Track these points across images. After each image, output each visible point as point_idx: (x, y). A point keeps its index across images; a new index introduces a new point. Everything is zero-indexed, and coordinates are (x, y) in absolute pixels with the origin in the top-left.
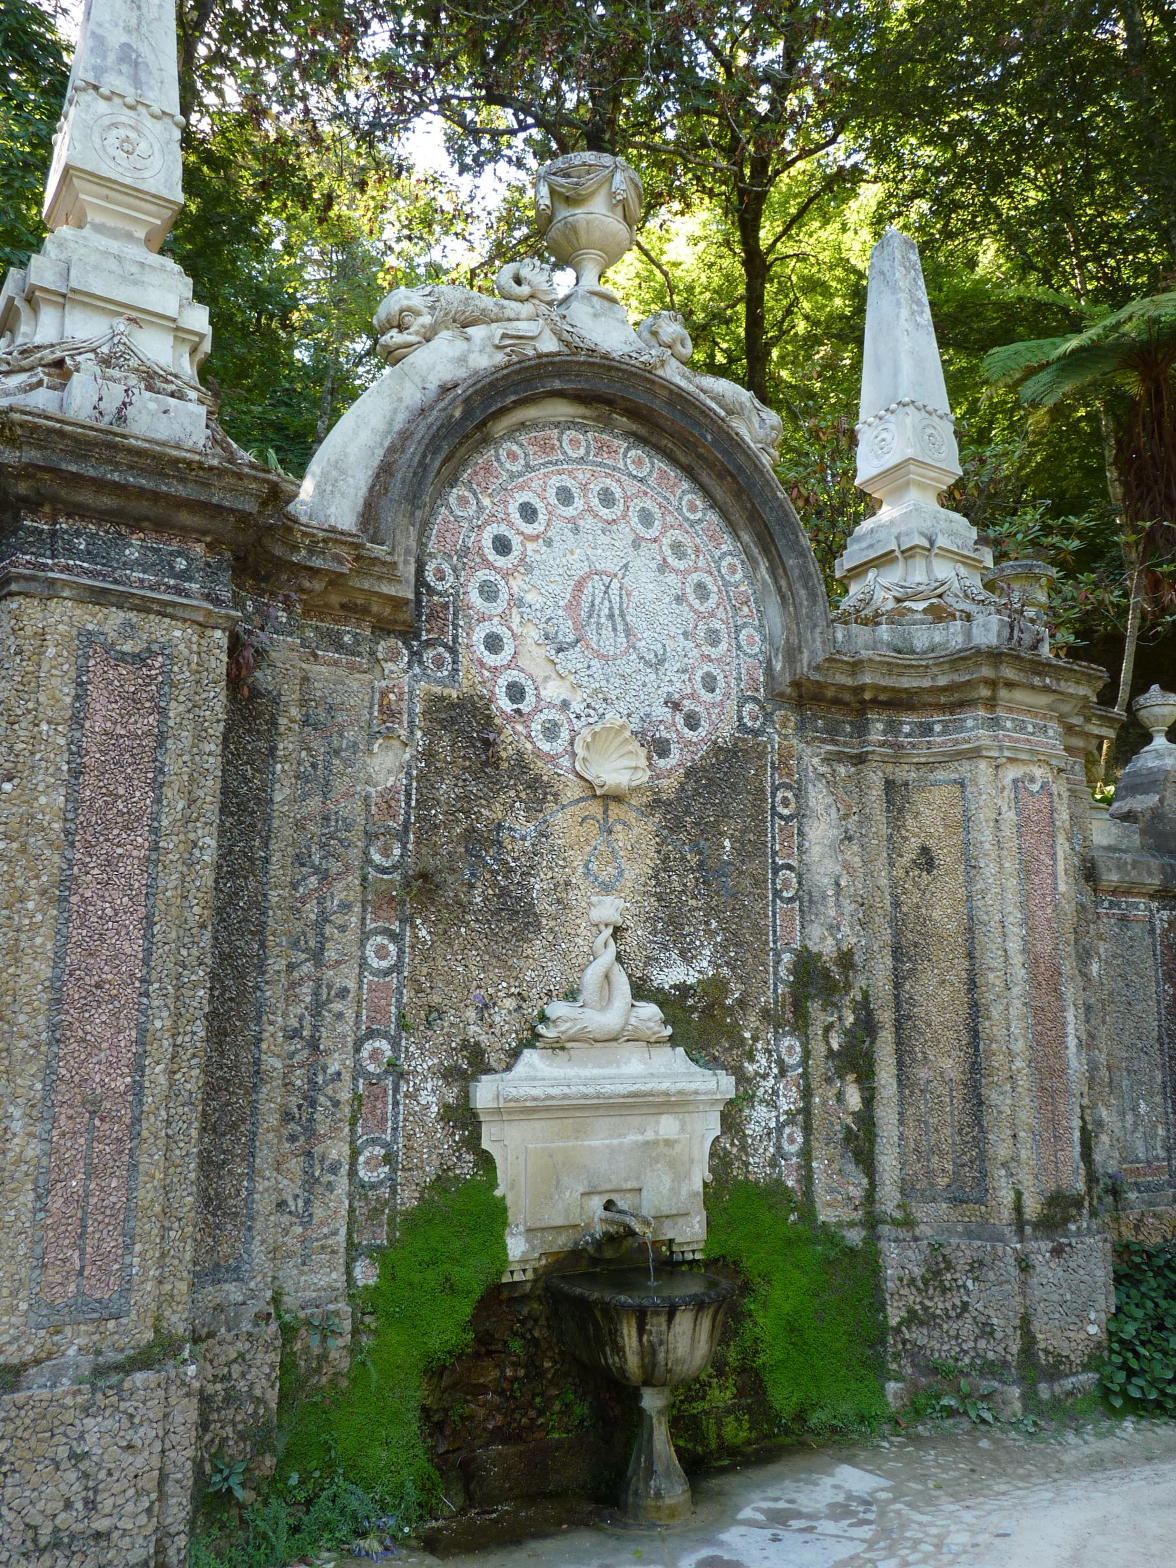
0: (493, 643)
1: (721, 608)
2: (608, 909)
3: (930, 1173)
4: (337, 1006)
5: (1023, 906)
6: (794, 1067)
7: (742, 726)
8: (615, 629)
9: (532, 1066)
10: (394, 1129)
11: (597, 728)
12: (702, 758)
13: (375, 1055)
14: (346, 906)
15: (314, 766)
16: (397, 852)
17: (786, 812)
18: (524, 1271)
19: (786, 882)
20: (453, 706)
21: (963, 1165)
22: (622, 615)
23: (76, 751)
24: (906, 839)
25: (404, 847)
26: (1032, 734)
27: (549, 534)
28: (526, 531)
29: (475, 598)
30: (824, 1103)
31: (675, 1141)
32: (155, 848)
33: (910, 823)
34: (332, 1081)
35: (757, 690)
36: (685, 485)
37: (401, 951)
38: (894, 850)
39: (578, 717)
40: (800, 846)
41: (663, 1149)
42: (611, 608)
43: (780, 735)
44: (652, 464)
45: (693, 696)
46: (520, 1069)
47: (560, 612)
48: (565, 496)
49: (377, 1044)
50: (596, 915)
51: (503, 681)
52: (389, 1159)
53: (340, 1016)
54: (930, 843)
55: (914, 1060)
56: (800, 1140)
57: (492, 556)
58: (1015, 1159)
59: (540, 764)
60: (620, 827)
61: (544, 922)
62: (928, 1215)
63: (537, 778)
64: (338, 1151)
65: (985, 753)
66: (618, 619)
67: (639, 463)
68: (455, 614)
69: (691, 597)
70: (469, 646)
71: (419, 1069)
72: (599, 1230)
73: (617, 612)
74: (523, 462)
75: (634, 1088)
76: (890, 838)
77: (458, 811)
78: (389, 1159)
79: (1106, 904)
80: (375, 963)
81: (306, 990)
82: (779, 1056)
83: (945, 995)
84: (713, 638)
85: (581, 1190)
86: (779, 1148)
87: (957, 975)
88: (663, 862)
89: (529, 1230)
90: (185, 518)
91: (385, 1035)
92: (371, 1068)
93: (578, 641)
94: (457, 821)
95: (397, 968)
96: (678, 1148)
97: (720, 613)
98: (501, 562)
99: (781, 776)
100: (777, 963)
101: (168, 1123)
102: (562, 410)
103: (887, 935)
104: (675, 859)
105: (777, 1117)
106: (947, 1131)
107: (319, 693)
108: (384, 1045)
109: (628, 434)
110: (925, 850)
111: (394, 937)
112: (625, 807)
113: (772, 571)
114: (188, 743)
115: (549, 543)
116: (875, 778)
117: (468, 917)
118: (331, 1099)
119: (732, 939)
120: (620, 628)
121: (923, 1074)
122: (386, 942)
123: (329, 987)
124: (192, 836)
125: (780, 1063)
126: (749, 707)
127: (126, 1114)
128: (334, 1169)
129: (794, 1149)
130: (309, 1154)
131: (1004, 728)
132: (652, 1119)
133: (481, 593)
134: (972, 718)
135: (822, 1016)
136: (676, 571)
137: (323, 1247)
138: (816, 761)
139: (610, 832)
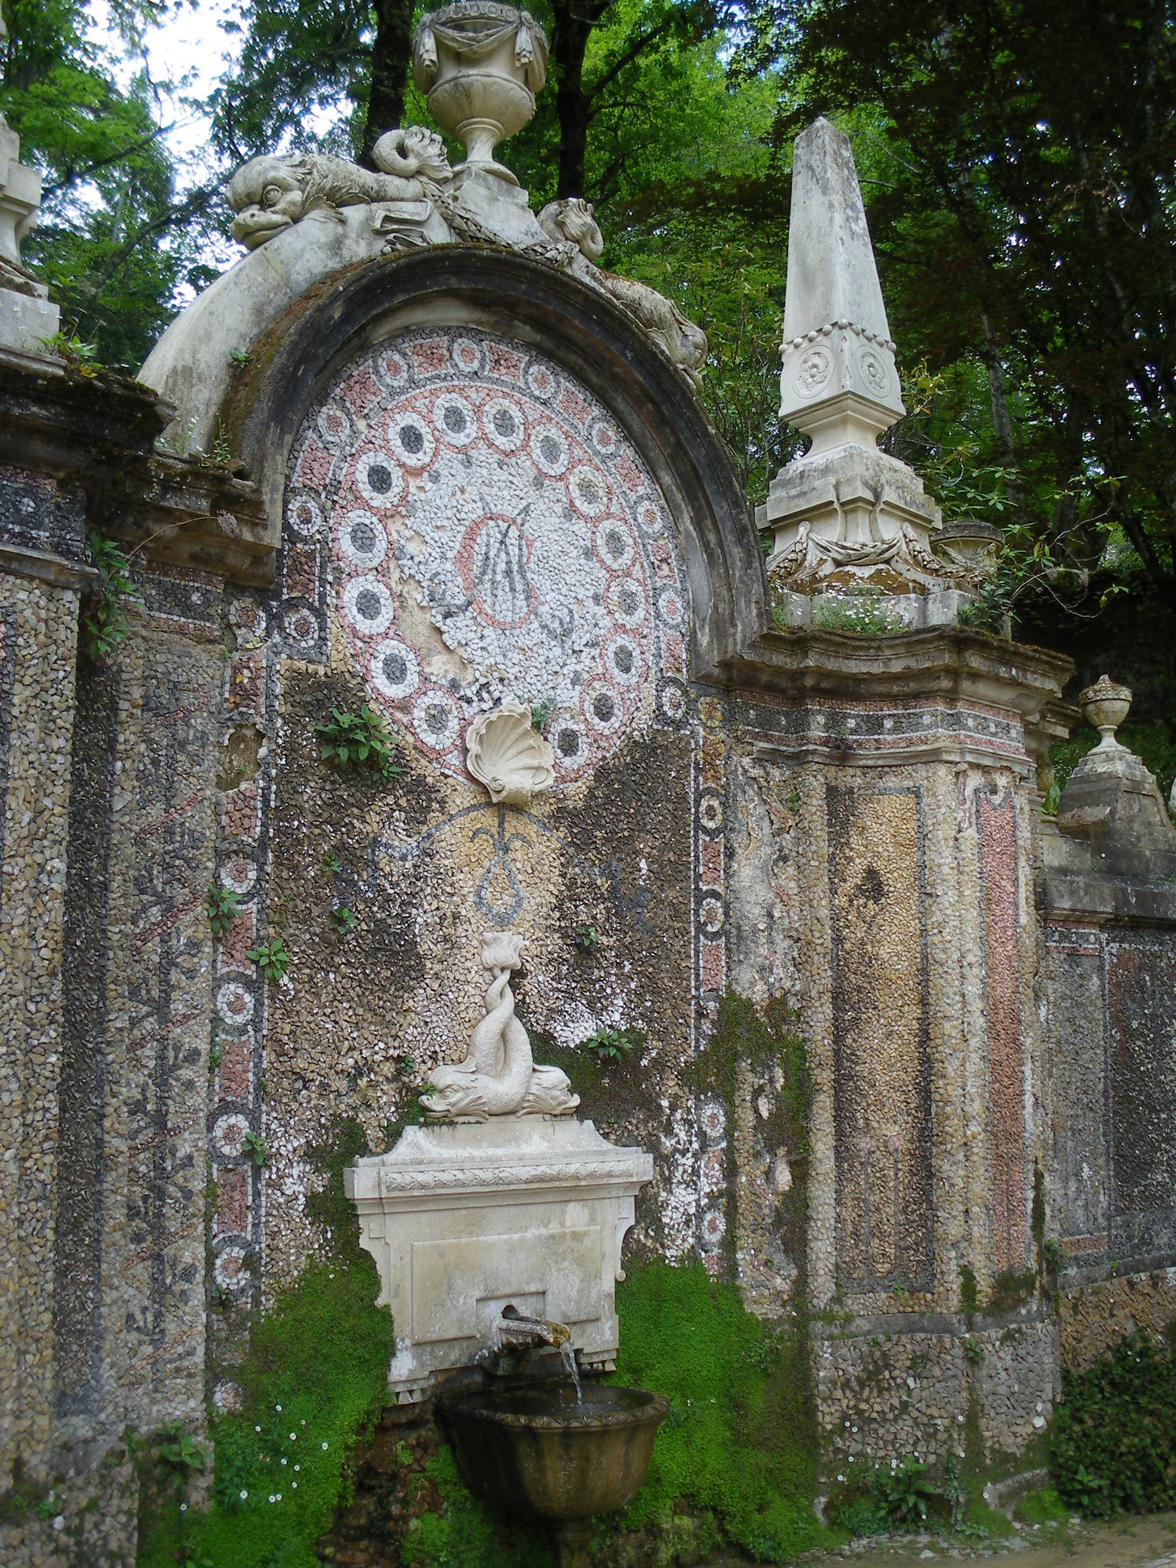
0: (368, 605)
1: (638, 566)
2: (506, 948)
3: (869, 1260)
4: (186, 1073)
5: (983, 941)
6: (717, 1141)
8: (513, 590)
9: (416, 1146)
10: (255, 1225)
11: (494, 716)
12: (615, 756)
13: (230, 1134)
15: (155, 763)
16: (253, 875)
17: (711, 825)
18: (411, 1392)
19: (711, 913)
20: (319, 686)
21: (907, 1248)
24: (850, 860)
25: (261, 869)
26: (995, 735)
27: (437, 466)
28: (408, 462)
29: (346, 546)
30: (751, 1182)
31: (585, 1234)
33: (855, 841)
34: (183, 1166)
35: (679, 670)
36: (596, 411)
37: (259, 1004)
38: (836, 874)
39: (469, 701)
40: (727, 868)
42: (509, 563)
43: (705, 727)
44: (558, 383)
45: (604, 677)
46: (402, 1150)
48: (455, 420)
49: (233, 1120)
50: (490, 955)
52: (250, 1263)
53: (190, 1085)
54: (879, 865)
55: (855, 1128)
56: (722, 1227)
57: (367, 492)
58: (968, 1238)
59: (424, 762)
60: (517, 844)
61: (429, 965)
62: (865, 1306)
63: (420, 781)
64: (192, 1253)
65: (945, 757)
66: (517, 577)
67: (542, 382)
69: (603, 551)
70: (337, 608)
71: (283, 1151)
72: (496, 1342)
73: (515, 568)
74: (405, 375)
75: (539, 1171)
76: (832, 858)
77: (327, 822)
78: (250, 1263)
79: (1056, 938)
80: (229, 1019)
81: (149, 1051)
82: (700, 1128)
83: (891, 1049)
85: (478, 1294)
86: (699, 1238)
88: (569, 888)
89: (417, 1345)
92: (226, 1150)
93: (470, 603)
94: (324, 835)
95: (256, 1022)
96: (587, 1242)
99: (706, 779)
101: (20, 1222)
102: (456, 314)
103: (826, 979)
104: (583, 885)
105: (698, 1201)
106: (890, 1210)
107: (161, 669)
109: (528, 346)
113: (698, 523)
114: (34, 738)
115: (435, 478)
116: (815, 784)
117: (337, 960)
118: (181, 1189)
119: (651, 986)
120: (519, 587)
121: (864, 1143)
122: (240, 991)
123: (177, 1049)
124: (39, 858)
125: (702, 1135)
126: (670, 691)
128: (188, 1274)
129: (715, 1238)
130: (158, 1257)
131: (965, 727)
132: (557, 1208)
133: (354, 539)
134: (931, 712)
135: (750, 1077)
136: (586, 518)
137: (178, 1370)
138: (746, 761)
139: (506, 850)
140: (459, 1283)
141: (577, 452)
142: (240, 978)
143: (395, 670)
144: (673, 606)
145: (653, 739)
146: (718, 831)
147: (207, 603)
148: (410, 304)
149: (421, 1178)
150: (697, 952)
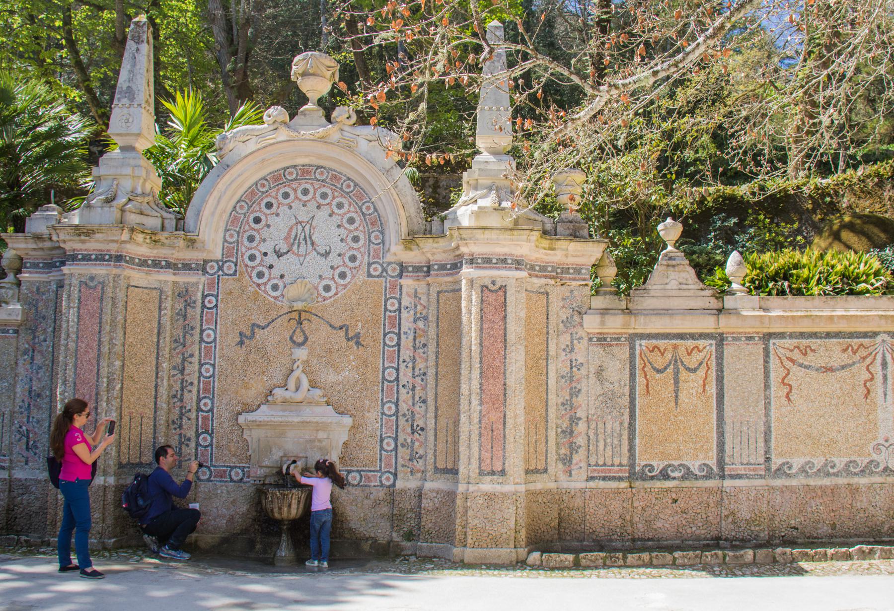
4: (189, 388)
8: (306, 243)
14: (192, 356)
22: (310, 237)
41: (317, 444)
53: (190, 391)
64: (191, 434)
66: (308, 239)
80: (205, 374)
95: (213, 376)
97: (361, 228)
98: (257, 226)
100: (383, 374)
108: (209, 402)
115: (278, 215)
120: (309, 243)
128: (189, 439)
140: (274, 450)
141: (336, 194)
150: (384, 352)
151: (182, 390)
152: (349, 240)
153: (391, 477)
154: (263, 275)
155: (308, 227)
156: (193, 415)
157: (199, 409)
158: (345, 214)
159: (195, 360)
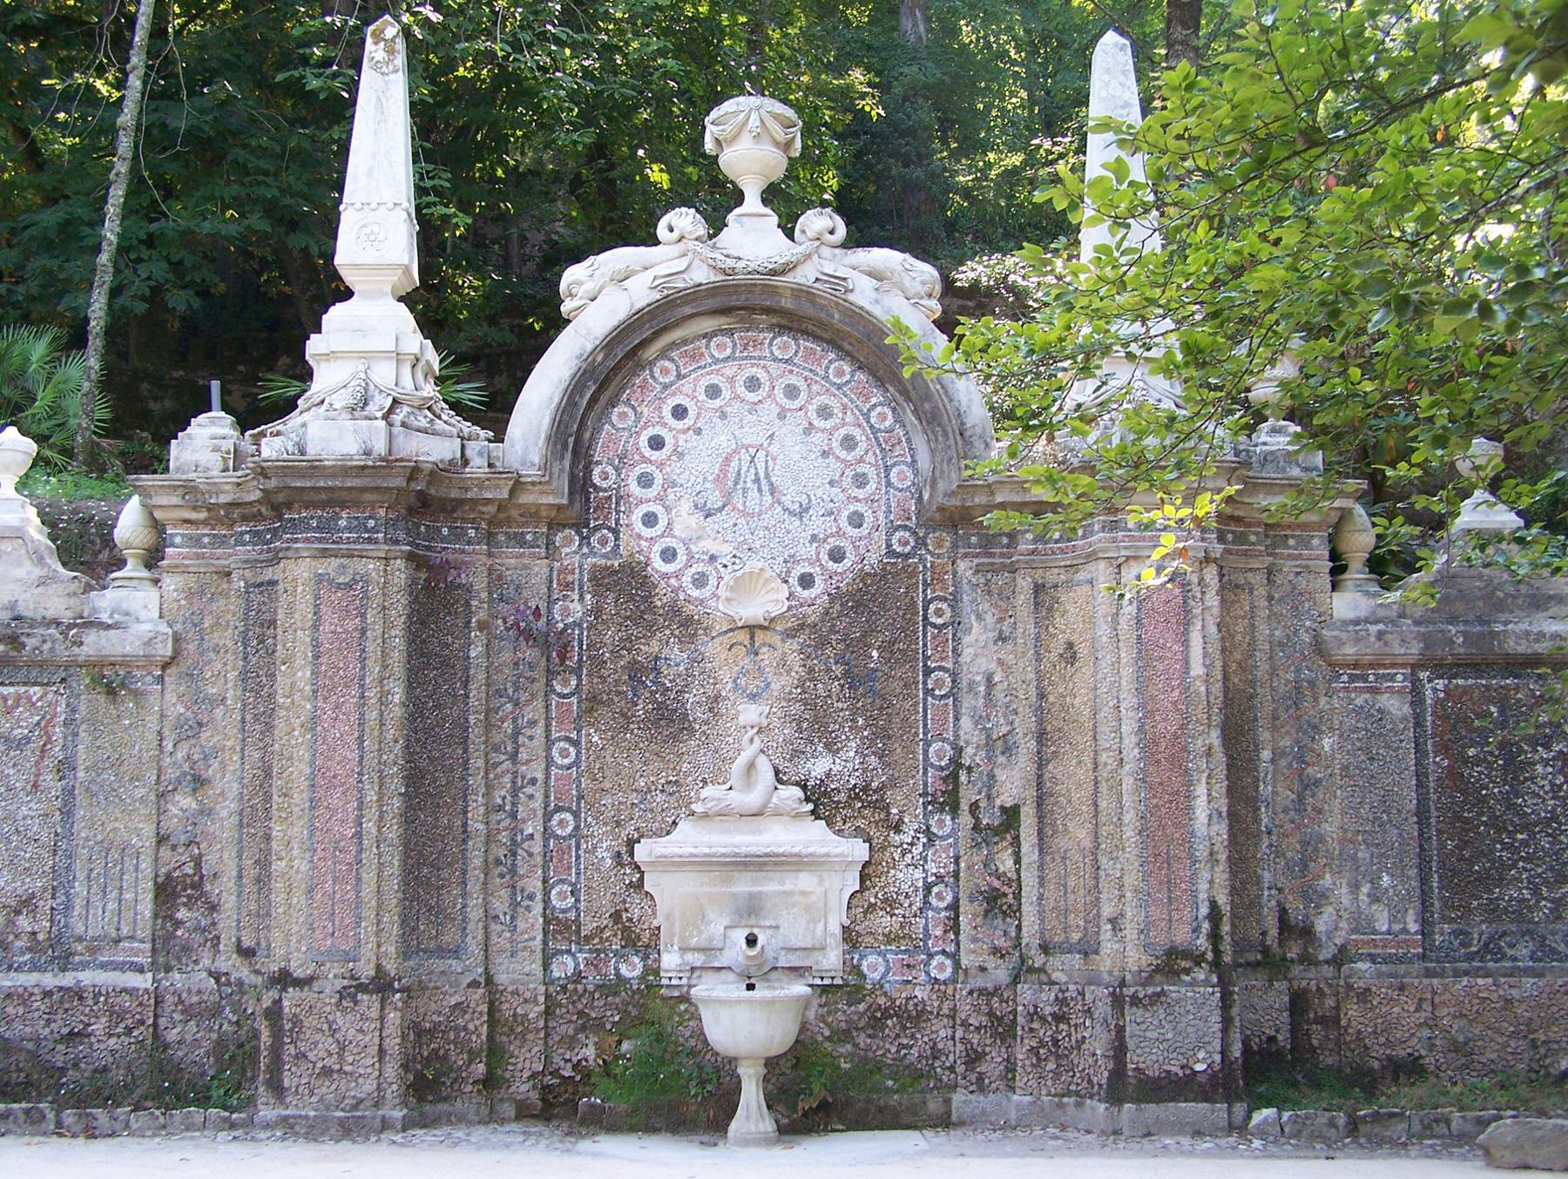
4: (529, 790)
6: (942, 838)
7: (891, 552)
8: (760, 490)
10: (578, 874)
11: (739, 574)
13: (562, 823)
14: (533, 723)
16: (574, 682)
17: (940, 621)
22: (767, 476)
23: (316, 644)
25: (580, 679)
29: (634, 488)
32: (363, 697)
35: (909, 519)
36: (832, 356)
37: (578, 753)
47: (708, 485)
48: (713, 392)
50: (742, 720)
51: (657, 548)
53: (531, 797)
64: (534, 884)
66: (764, 482)
67: (785, 347)
68: (617, 503)
73: (762, 476)
79: (1345, 678)
81: (507, 779)
84: (860, 480)
86: (926, 902)
87: (1087, 760)
90: (368, 497)
91: (569, 810)
95: (577, 763)
96: (813, 898)
97: (870, 458)
98: (655, 455)
99: (934, 591)
100: (926, 752)
102: (709, 324)
105: (925, 879)
108: (568, 816)
109: (771, 328)
110: (1070, 645)
111: (576, 743)
112: (769, 634)
115: (698, 432)
116: (1024, 583)
120: (765, 488)
123: (523, 778)
126: (898, 535)
127: (353, 849)
128: (531, 897)
129: (942, 905)
130: (514, 887)
140: (712, 915)
141: (815, 388)
142: (567, 739)
143: (669, 555)
144: (901, 476)
145: (883, 569)
146: (945, 625)
147: (535, 539)
148: (657, 334)
149: (677, 851)
150: (925, 711)
151: (515, 794)
152: (847, 481)
153: (948, 962)
154: (675, 554)
155: (761, 454)
156: (537, 847)
157: (547, 833)
158: (836, 428)
159: (539, 731)
